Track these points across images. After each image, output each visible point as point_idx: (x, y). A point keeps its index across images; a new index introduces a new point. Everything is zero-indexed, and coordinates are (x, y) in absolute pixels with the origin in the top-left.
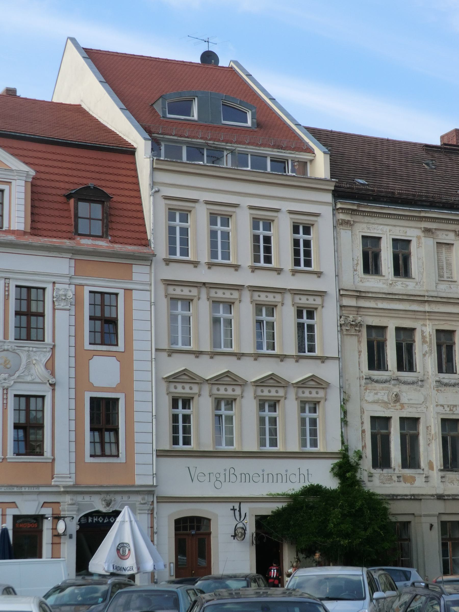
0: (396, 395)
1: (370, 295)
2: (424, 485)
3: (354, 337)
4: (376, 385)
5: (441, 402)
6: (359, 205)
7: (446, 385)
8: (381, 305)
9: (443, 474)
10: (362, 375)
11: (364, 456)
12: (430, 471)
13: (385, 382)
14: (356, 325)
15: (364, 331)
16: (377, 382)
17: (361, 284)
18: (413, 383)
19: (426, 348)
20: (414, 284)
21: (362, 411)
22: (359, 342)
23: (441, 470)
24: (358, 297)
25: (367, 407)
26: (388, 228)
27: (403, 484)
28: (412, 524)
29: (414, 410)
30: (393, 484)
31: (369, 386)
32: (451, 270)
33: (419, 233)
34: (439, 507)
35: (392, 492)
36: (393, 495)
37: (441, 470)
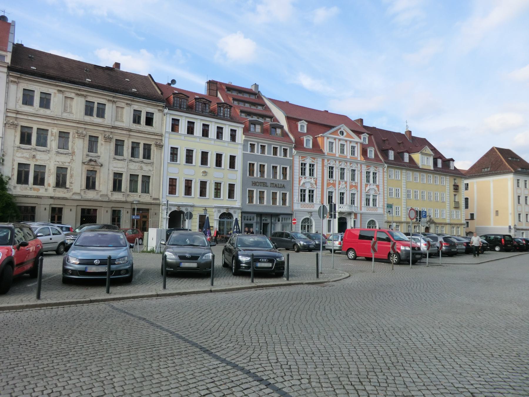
0: (34, 155)
1: (24, 113)
2: (45, 192)
3: (12, 130)
4: (23, 150)
5: (58, 160)
6: (20, 75)
7: (61, 154)
8: (30, 118)
9: (54, 188)
10: (15, 145)
11: (12, 179)
12: (49, 188)
13: (29, 149)
14: (13, 125)
15: (19, 129)
16: (23, 149)
17: (20, 108)
18: (44, 151)
19: (53, 138)
20: (50, 112)
21: (13, 160)
22: (16, 132)
23: (53, 187)
24: (17, 113)
25: (15, 158)
26: (39, 87)
27: (33, 191)
28: (37, 208)
29: (43, 162)
30: (28, 191)
31: (19, 150)
32: (72, 108)
33: (56, 91)
34: (51, 201)
35: (27, 194)
36: (26, 195)
37: (53, 187)
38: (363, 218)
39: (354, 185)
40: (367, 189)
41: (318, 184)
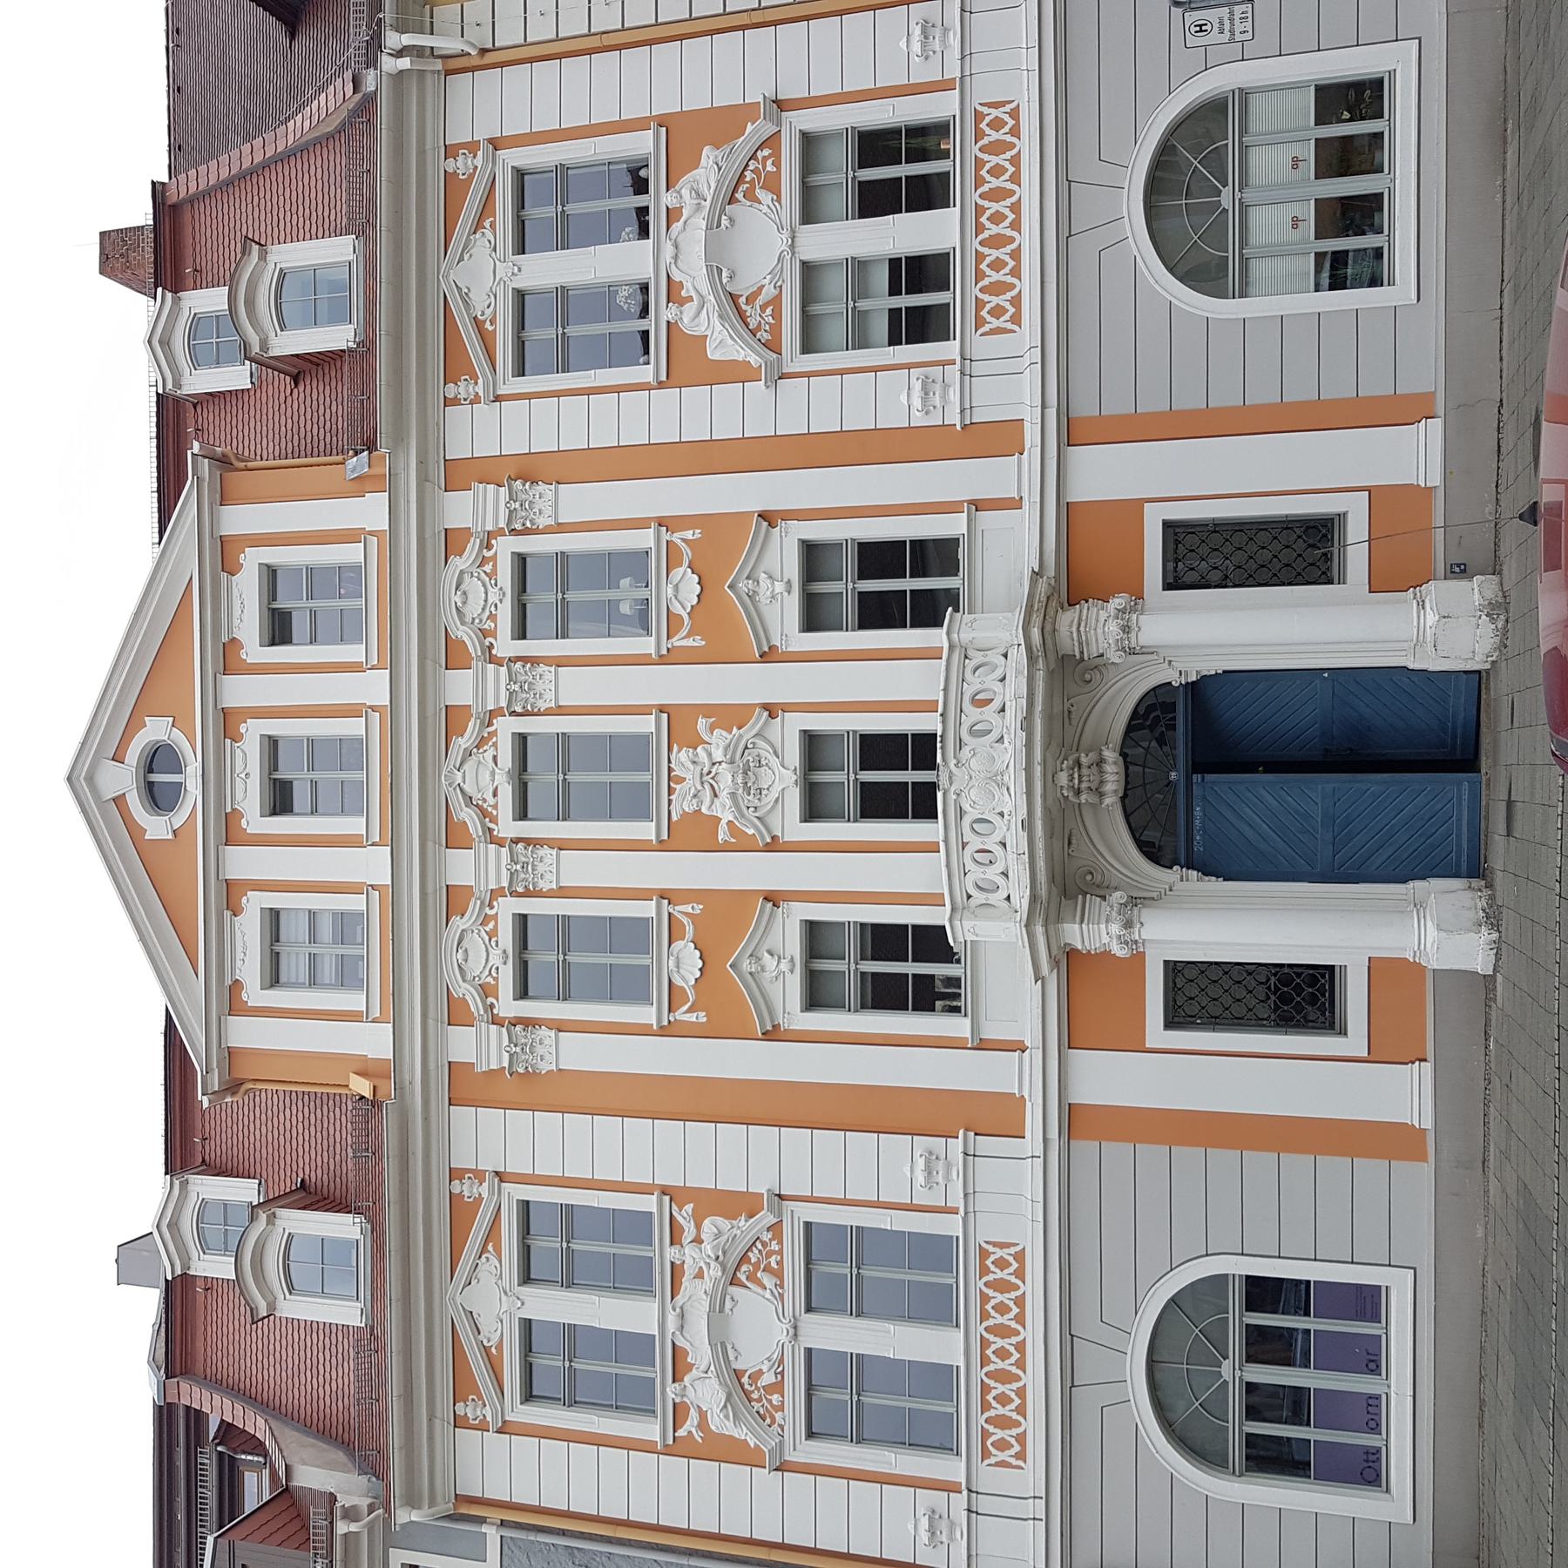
38: (1118, 404)
39: (691, 588)
40: (724, 344)
41: (732, 1181)
